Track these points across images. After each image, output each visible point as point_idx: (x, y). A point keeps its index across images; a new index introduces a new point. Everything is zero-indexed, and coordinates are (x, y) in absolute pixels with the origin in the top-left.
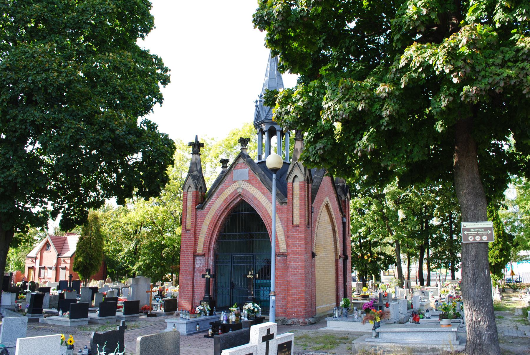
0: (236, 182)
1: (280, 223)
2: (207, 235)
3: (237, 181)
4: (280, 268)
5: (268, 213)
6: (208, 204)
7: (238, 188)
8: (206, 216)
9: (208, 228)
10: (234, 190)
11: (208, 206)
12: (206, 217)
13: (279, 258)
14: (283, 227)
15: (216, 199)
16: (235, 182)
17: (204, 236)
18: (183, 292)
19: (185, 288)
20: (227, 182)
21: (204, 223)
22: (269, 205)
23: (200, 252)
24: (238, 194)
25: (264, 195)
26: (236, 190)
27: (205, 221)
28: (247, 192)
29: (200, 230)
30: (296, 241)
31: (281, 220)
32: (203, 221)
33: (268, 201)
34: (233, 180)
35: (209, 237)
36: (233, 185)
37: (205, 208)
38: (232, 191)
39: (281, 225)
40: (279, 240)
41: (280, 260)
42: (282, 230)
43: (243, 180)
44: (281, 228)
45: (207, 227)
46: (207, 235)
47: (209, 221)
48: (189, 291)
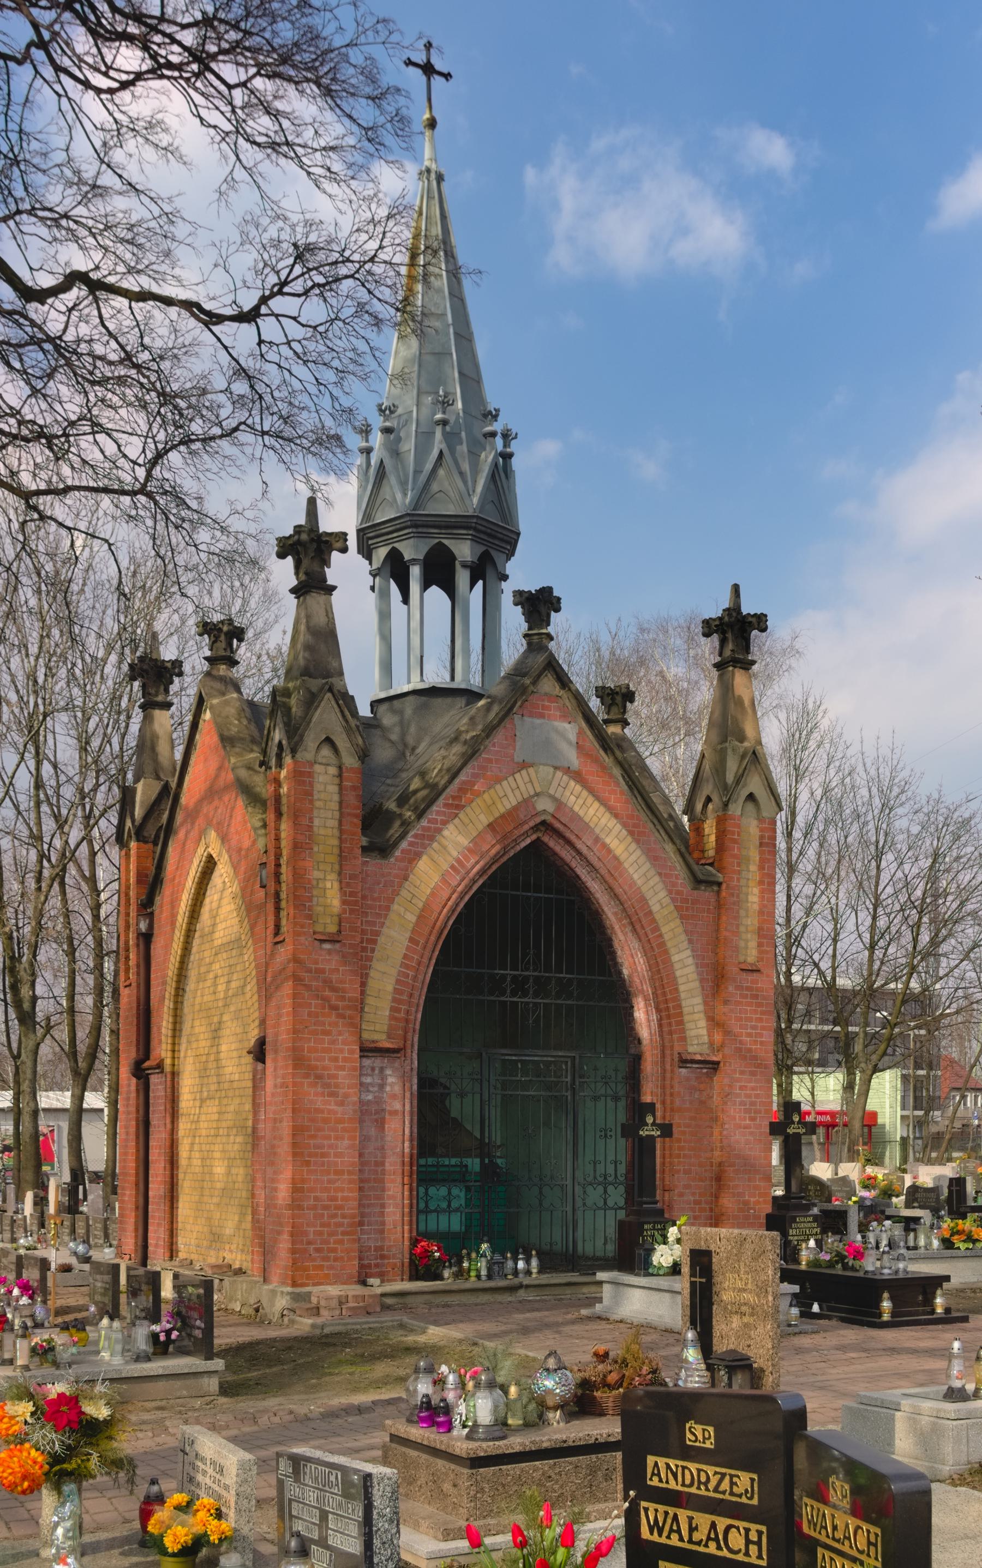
0: (531, 770)
1: (688, 952)
2: (407, 967)
3: (531, 765)
4: (688, 1105)
5: (650, 913)
6: (409, 838)
7: (537, 795)
8: (400, 885)
9: (411, 940)
10: (520, 799)
11: (411, 844)
12: (404, 893)
13: (683, 1070)
14: (697, 965)
15: (445, 823)
16: (524, 765)
17: (394, 972)
18: (314, 1208)
19: (327, 1190)
20: (490, 761)
21: (392, 915)
22: (652, 883)
23: (376, 1037)
24: (538, 820)
25: (637, 842)
26: (527, 802)
27: (395, 907)
28: (576, 817)
29: (375, 942)
30: (750, 1019)
31: (690, 941)
32: (388, 908)
33: (648, 865)
34: (518, 758)
35: (415, 978)
36: (517, 776)
37: (398, 853)
38: (514, 803)
39: (690, 961)
40: (686, 1010)
41: (688, 1079)
42: (695, 976)
43: (556, 768)
44: (692, 969)
45: (408, 935)
46: (407, 967)
47: (417, 912)
48: (345, 1199)
